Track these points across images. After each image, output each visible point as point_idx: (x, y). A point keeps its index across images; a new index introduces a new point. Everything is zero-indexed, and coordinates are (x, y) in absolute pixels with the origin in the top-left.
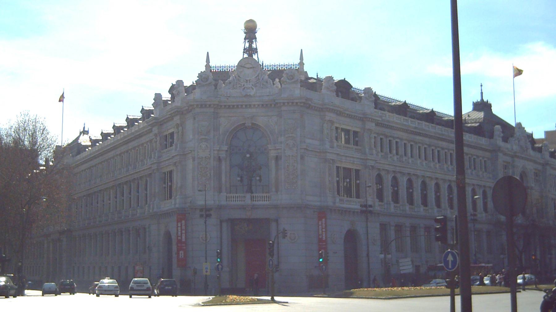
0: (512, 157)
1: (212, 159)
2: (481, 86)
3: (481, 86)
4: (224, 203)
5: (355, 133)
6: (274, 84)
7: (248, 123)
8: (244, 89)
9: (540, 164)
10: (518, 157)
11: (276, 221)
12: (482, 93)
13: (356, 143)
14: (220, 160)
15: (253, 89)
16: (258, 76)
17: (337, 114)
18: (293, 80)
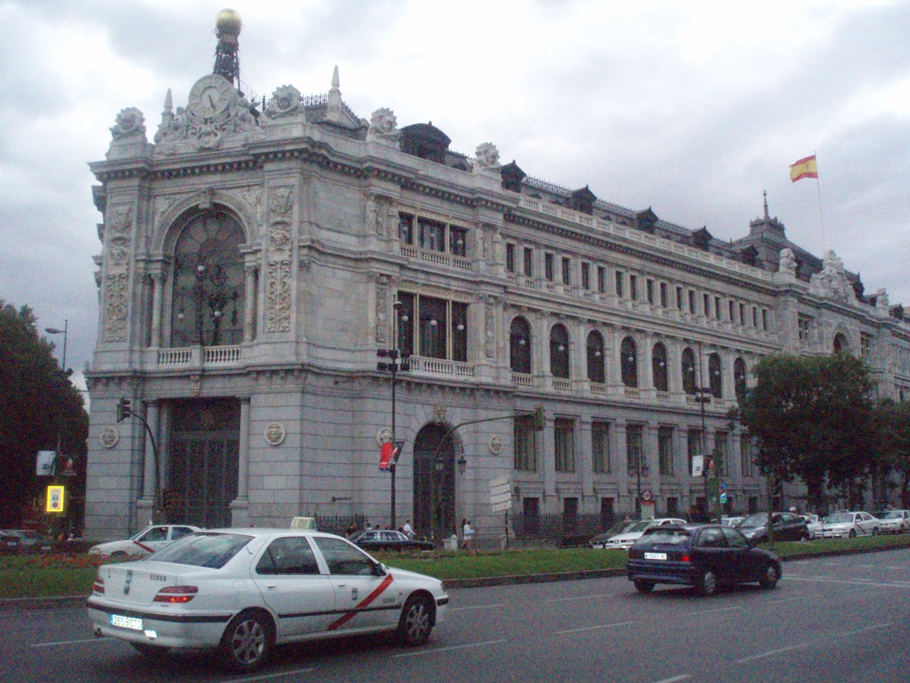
0: (818, 307)
1: (131, 278)
2: (765, 194)
3: (765, 194)
4: (151, 367)
5: (459, 232)
6: (257, 122)
7: (204, 203)
8: (200, 137)
9: (872, 324)
10: (830, 308)
11: (248, 400)
12: (766, 206)
13: (459, 250)
14: (149, 281)
15: (216, 135)
16: (227, 108)
17: (404, 187)
18: (290, 108)
